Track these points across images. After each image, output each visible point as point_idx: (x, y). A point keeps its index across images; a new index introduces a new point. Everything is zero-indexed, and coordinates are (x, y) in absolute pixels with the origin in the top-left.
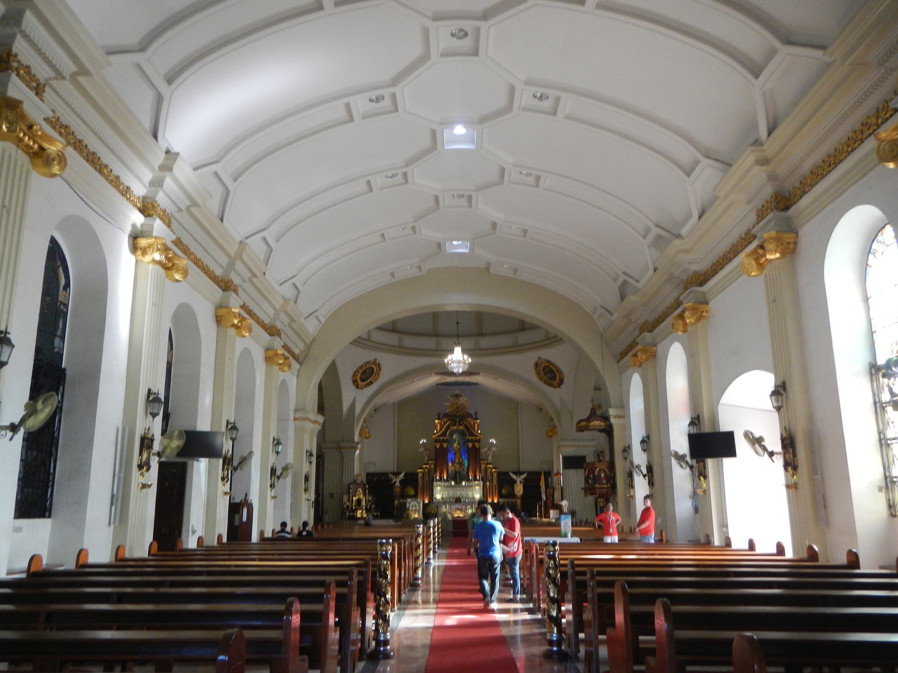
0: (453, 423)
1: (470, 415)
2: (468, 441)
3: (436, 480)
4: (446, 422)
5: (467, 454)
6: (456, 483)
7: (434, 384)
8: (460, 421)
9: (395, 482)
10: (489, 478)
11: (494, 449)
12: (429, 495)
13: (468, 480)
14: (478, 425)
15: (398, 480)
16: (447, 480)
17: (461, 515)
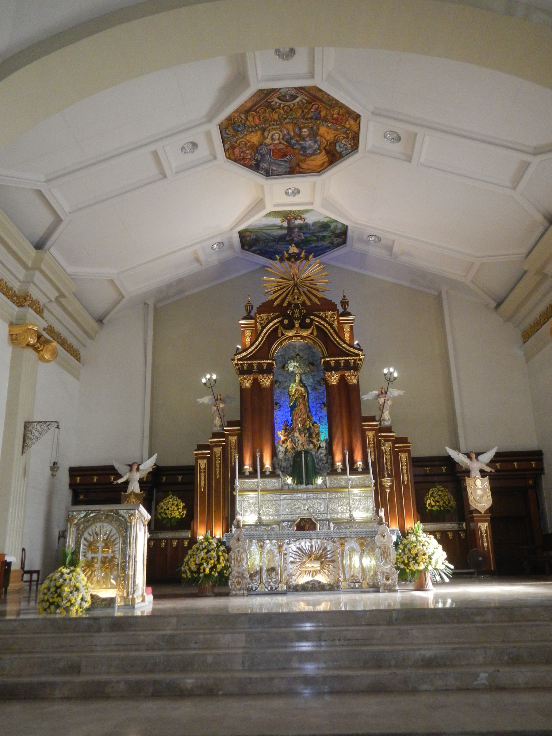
0: (286, 322)
1: (329, 305)
2: (328, 367)
3: (242, 475)
4: (268, 323)
5: (324, 411)
6: (300, 482)
7: (236, 239)
8: (305, 316)
9: (127, 483)
10: (388, 466)
11: (394, 392)
12: (226, 519)
13: (333, 471)
14: (351, 328)
15: (137, 476)
16: (273, 474)
17: (322, 578)
